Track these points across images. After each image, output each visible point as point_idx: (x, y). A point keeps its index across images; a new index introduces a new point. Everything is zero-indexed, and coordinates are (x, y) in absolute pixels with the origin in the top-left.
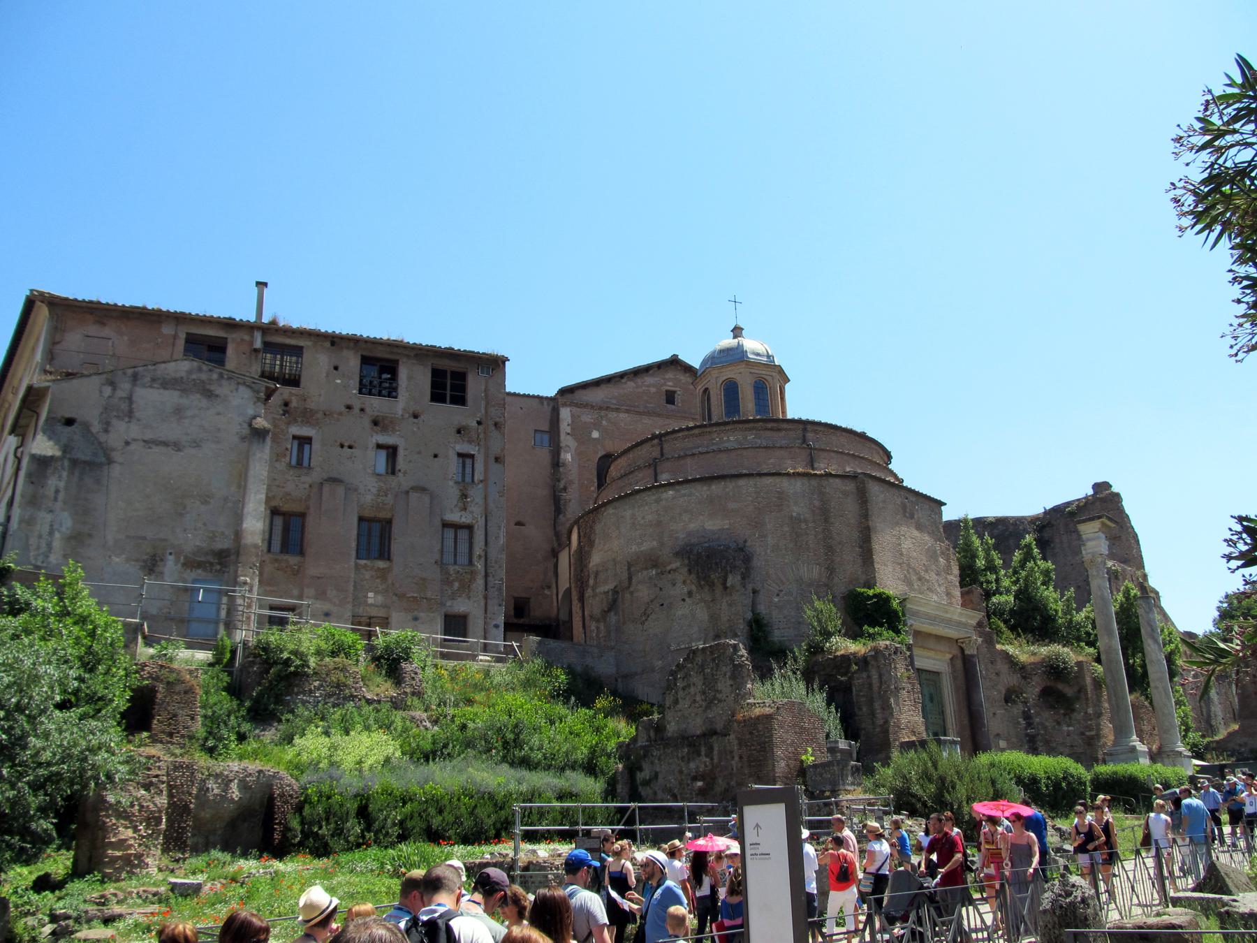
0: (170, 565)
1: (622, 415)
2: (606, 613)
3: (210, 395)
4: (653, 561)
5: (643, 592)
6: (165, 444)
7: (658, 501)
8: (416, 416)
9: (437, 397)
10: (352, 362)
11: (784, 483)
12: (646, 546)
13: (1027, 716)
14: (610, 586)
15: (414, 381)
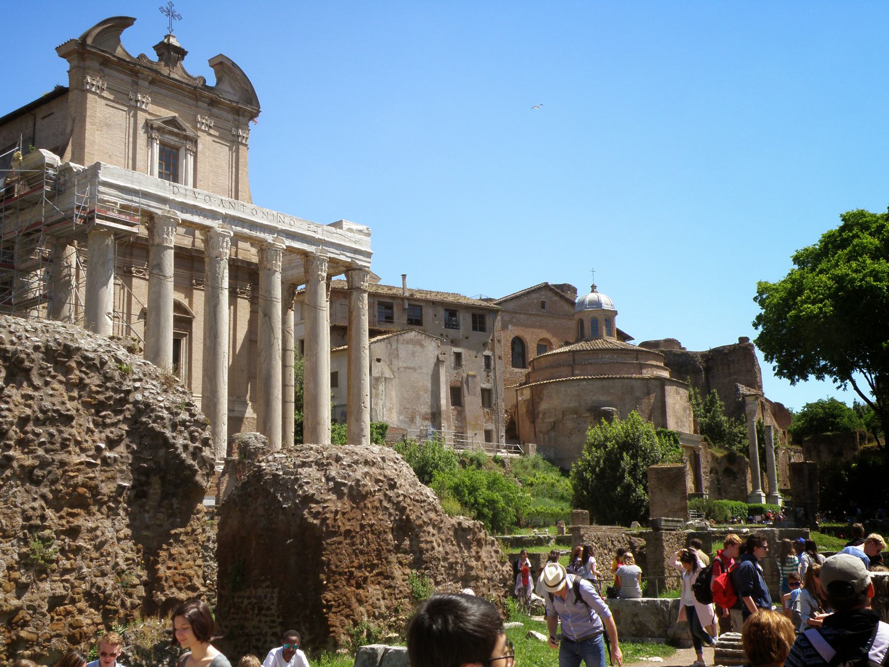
0: (418, 420)
1: (522, 316)
2: (548, 431)
3: (422, 346)
4: (575, 411)
5: (569, 424)
6: (410, 368)
7: (579, 385)
8: (467, 338)
9: (475, 329)
10: (442, 313)
11: (634, 382)
12: (572, 405)
13: (718, 480)
14: (552, 420)
15: (465, 320)
